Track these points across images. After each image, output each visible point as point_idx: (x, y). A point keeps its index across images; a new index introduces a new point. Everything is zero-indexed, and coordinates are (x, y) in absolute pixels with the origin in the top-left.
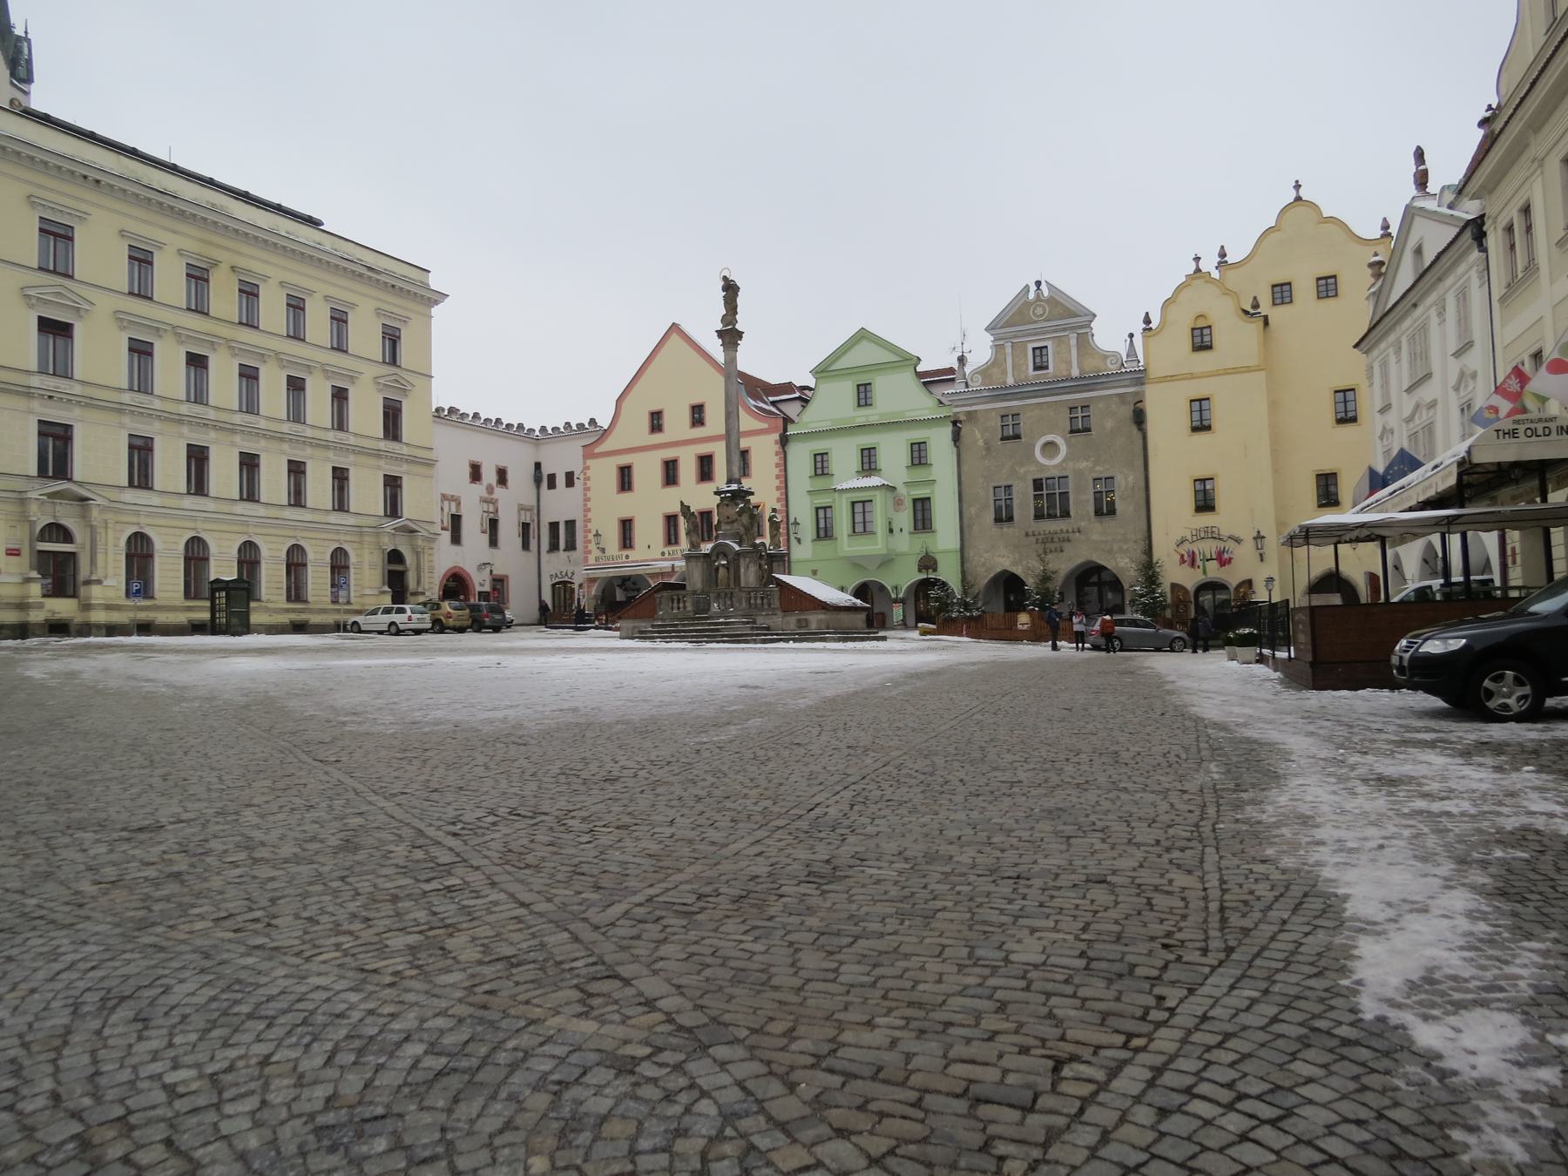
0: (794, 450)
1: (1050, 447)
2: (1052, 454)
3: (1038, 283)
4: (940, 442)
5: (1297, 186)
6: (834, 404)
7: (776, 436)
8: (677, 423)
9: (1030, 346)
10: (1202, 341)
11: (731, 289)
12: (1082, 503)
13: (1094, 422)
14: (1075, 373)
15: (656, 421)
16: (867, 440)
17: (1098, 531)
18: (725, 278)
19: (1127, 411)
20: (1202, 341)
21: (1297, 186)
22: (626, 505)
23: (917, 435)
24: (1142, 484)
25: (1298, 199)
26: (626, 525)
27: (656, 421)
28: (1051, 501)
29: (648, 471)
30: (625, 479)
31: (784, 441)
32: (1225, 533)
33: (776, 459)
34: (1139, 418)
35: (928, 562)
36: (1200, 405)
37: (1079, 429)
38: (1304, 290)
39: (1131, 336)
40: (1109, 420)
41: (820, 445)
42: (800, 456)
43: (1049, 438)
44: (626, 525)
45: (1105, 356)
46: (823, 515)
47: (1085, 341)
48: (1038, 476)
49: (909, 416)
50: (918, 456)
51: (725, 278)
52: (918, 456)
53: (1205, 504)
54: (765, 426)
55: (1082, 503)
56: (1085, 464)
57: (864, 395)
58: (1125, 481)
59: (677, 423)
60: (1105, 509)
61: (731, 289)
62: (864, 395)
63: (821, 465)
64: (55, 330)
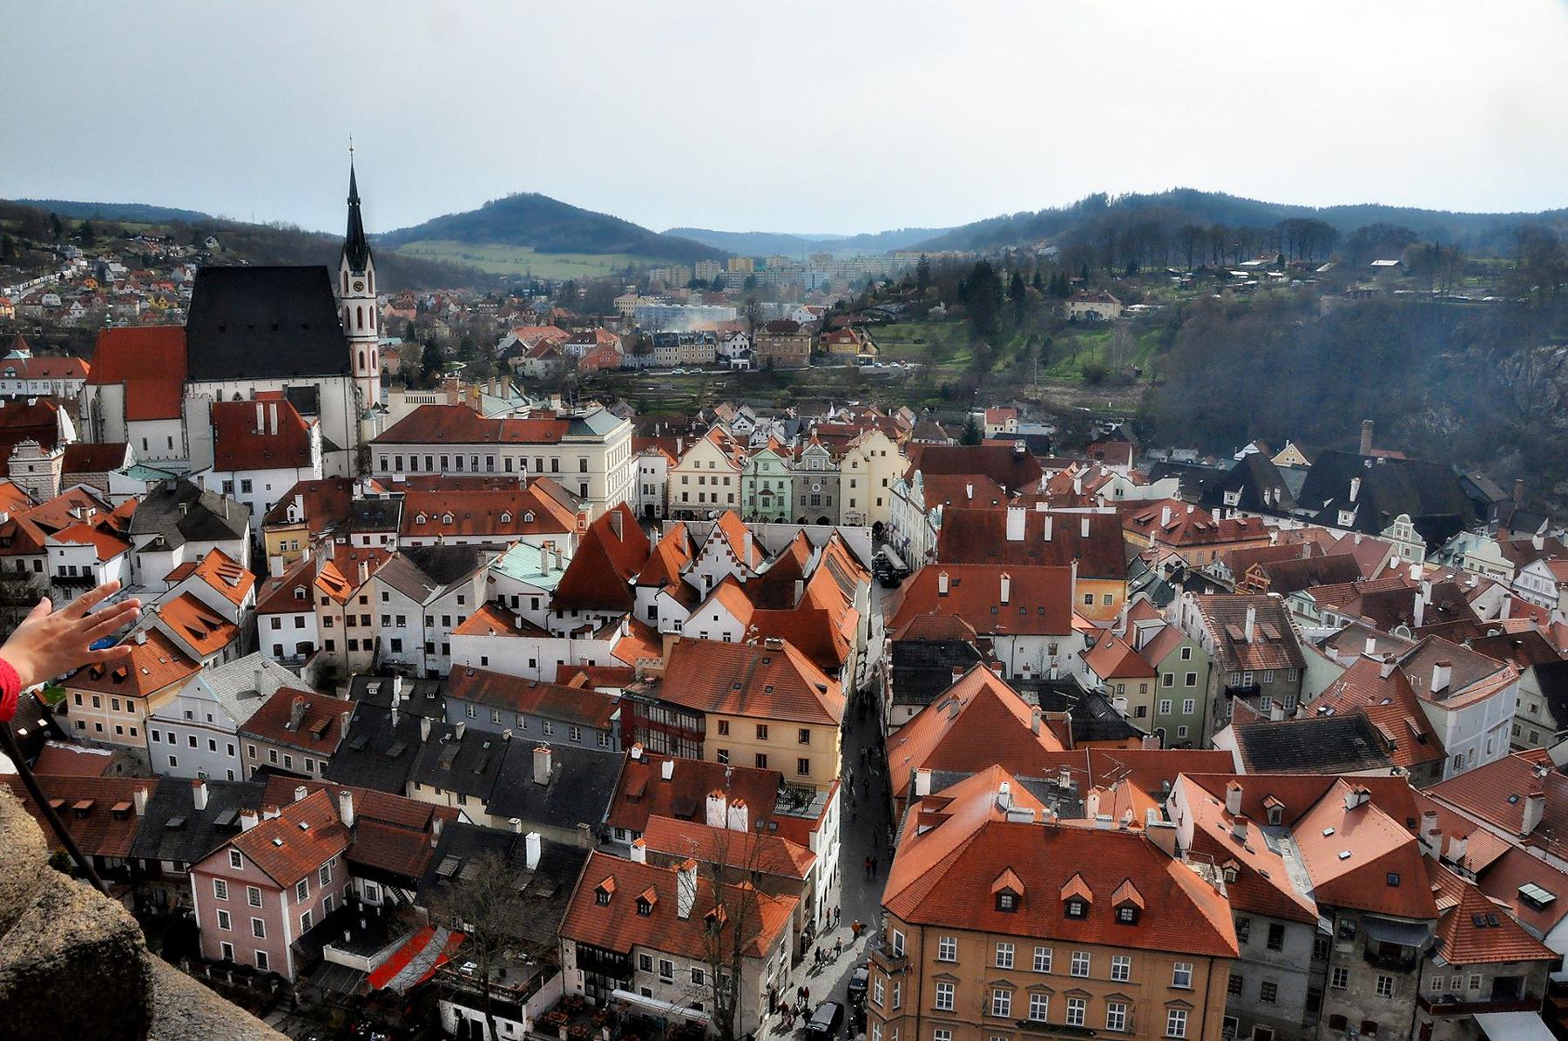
2: (817, 488)
4: (787, 483)
8: (705, 466)
10: (855, 465)
15: (697, 464)
20: (855, 465)
22: (685, 488)
26: (685, 496)
27: (697, 464)
28: (816, 500)
29: (694, 479)
30: (685, 481)
35: (782, 514)
38: (878, 453)
40: (830, 482)
44: (685, 496)
46: (752, 500)
50: (781, 485)
52: (781, 485)
53: (853, 505)
55: (823, 501)
59: (705, 466)
60: (829, 503)
64: (583, 469)
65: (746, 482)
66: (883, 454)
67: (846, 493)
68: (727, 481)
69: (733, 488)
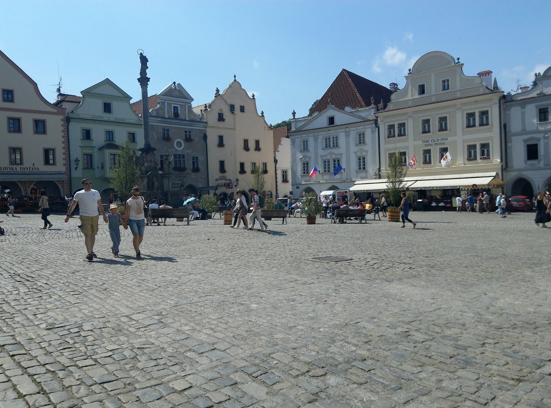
0: (72, 125)
1: (179, 144)
3: (174, 83)
5: (235, 77)
6: (95, 108)
7: (62, 117)
9: (173, 105)
10: (221, 118)
11: (144, 60)
12: (189, 165)
13: (192, 137)
14: (187, 119)
16: (110, 128)
17: (193, 175)
18: (141, 54)
19: (202, 135)
20: (221, 118)
21: (235, 77)
23: (132, 130)
24: (206, 160)
25: (235, 80)
31: (68, 120)
32: (228, 178)
33: (62, 128)
34: (205, 137)
36: (221, 138)
37: (188, 139)
39: (201, 110)
40: (197, 138)
41: (87, 126)
42: (76, 129)
43: (179, 140)
45: (196, 116)
47: (190, 107)
48: (176, 153)
49: (127, 121)
51: (141, 54)
54: (56, 111)
55: (189, 165)
56: (189, 151)
57: (107, 108)
58: (201, 158)
61: (144, 60)
62: (107, 108)
63: (87, 135)
65: (76, 129)
66: (242, 109)
67: (215, 155)
68: (40, 127)
69: (54, 137)
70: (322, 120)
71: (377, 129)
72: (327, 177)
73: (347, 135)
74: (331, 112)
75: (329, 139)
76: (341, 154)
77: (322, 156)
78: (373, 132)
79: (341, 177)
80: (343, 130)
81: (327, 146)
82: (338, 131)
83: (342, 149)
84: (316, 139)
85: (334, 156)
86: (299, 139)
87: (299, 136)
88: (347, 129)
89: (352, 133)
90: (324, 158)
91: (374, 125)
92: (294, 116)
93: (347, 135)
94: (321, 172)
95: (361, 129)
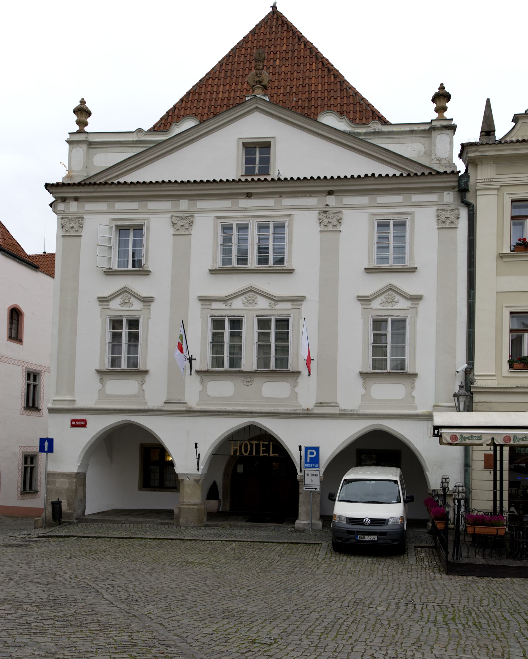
70: (216, 155)
71: (464, 213)
72: (223, 390)
73: (330, 222)
74: (257, 125)
75: (243, 228)
76: (297, 300)
77: (204, 300)
78: (445, 224)
79: (294, 395)
80: (312, 201)
81: (231, 263)
82: (287, 202)
83: (304, 276)
84: (183, 225)
85: (263, 304)
86: (105, 219)
87: (102, 206)
88: (331, 200)
89: (347, 216)
90: (219, 309)
91: (449, 197)
92: (82, 123)
93: (330, 222)
94: (196, 366)
95: (391, 204)
